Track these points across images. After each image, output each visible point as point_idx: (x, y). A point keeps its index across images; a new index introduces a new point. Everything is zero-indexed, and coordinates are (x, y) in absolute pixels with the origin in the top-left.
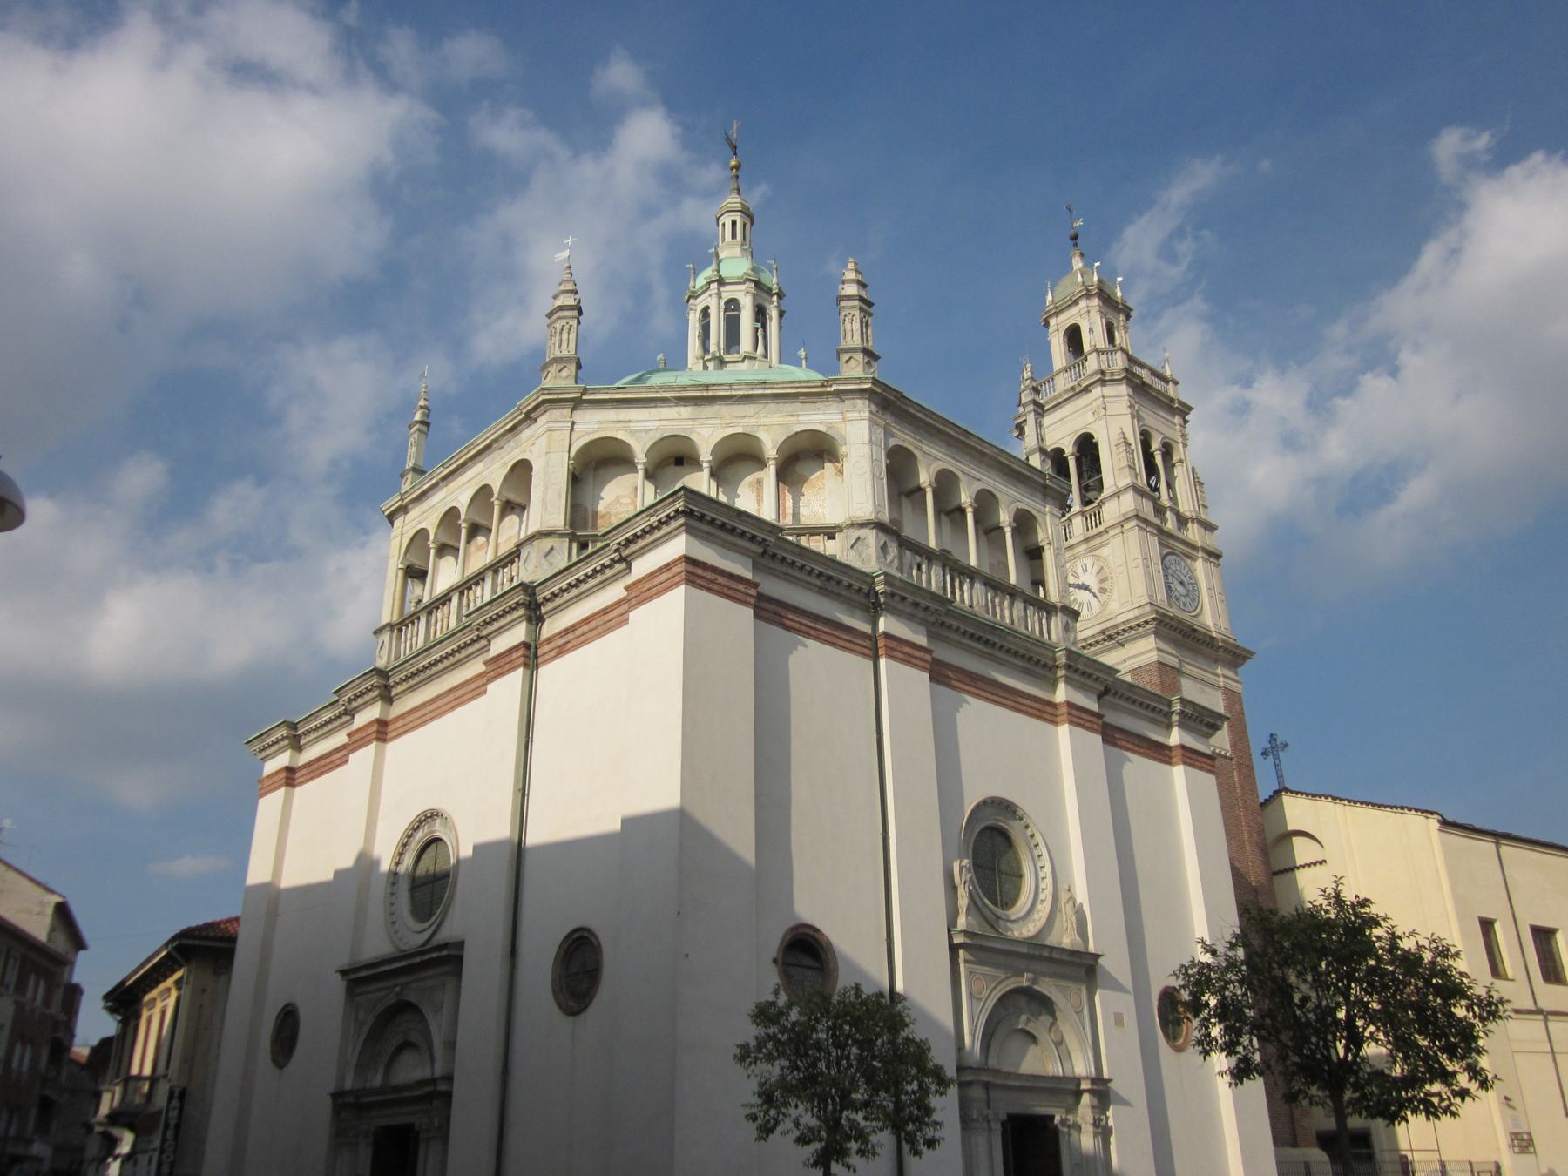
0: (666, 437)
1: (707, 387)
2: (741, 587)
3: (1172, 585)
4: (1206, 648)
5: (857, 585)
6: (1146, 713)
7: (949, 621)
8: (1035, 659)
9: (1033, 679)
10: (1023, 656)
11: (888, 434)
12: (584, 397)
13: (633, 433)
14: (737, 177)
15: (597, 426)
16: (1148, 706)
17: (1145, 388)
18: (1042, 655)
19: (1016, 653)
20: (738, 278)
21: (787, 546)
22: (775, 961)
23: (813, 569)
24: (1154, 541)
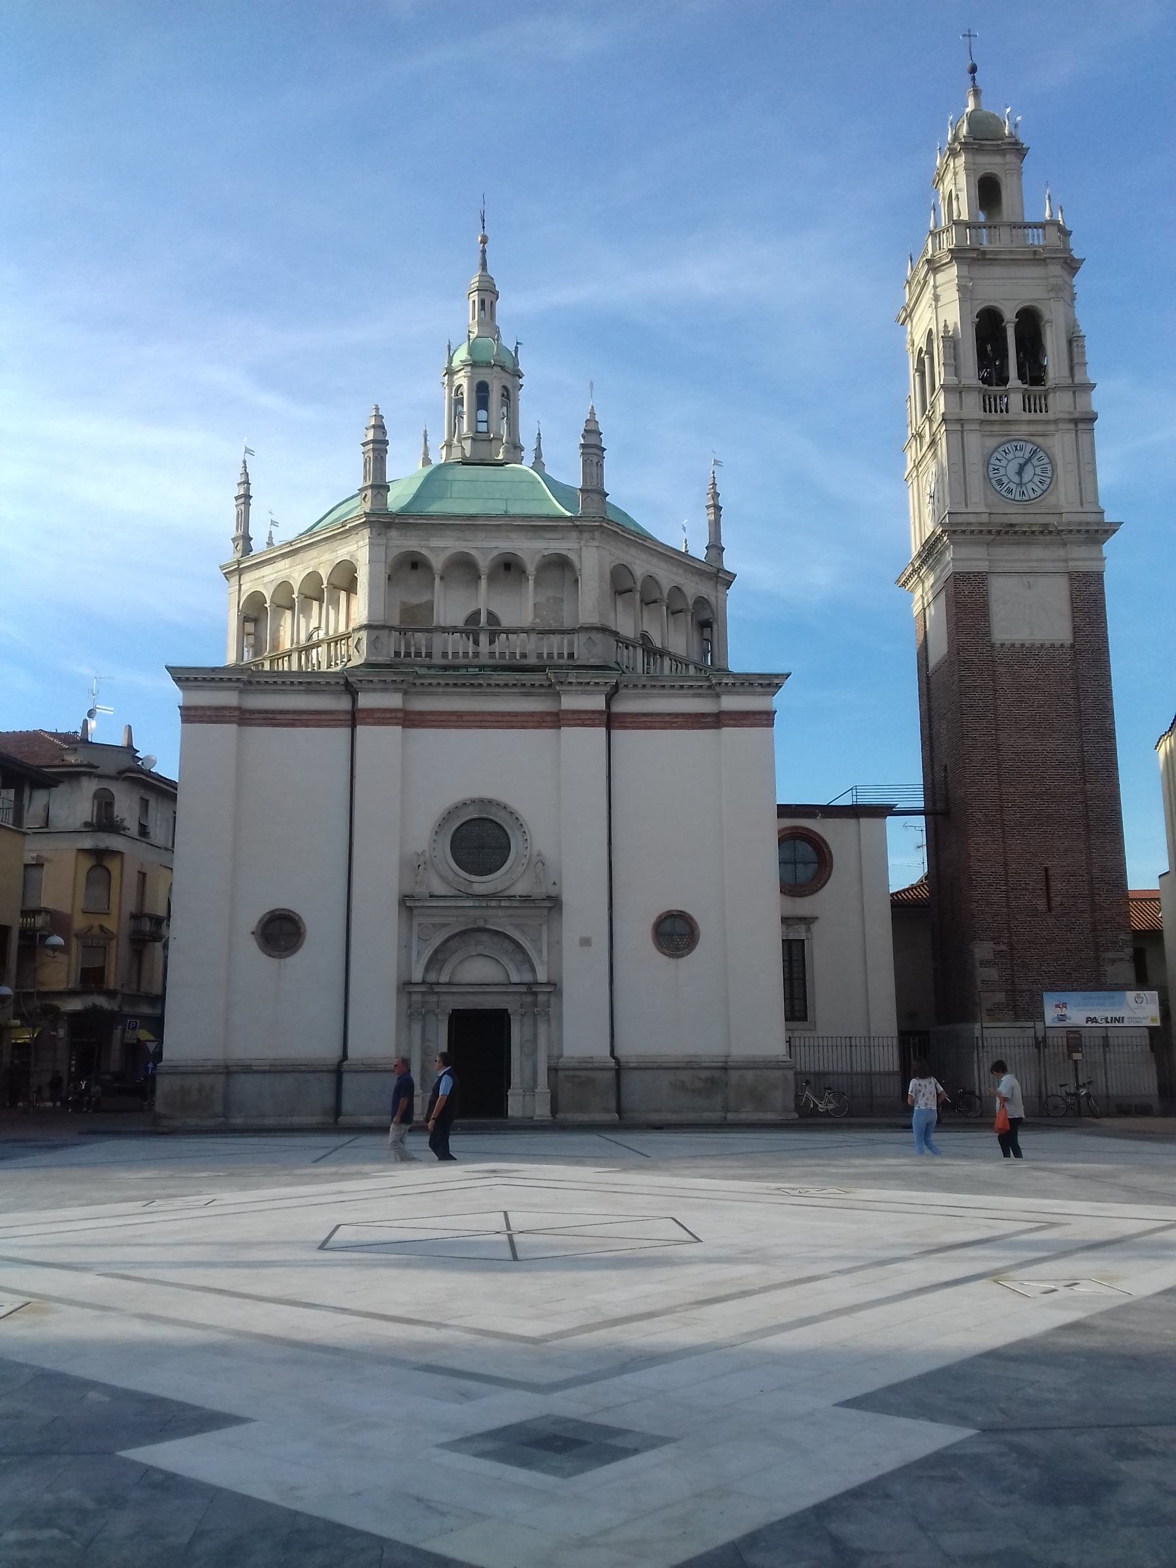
0: (280, 583)
1: (290, 544)
2: (227, 713)
3: (1005, 480)
4: (1042, 537)
5: (333, 681)
6: (681, 692)
7: (426, 681)
8: (528, 684)
9: (534, 697)
10: (516, 685)
11: (387, 547)
12: (241, 566)
13: (265, 585)
14: (484, 252)
15: (249, 584)
16: (682, 687)
17: (988, 257)
18: (532, 680)
19: (506, 685)
20: (460, 365)
21: (264, 674)
22: (253, 933)
23: (292, 683)
24: (973, 440)
